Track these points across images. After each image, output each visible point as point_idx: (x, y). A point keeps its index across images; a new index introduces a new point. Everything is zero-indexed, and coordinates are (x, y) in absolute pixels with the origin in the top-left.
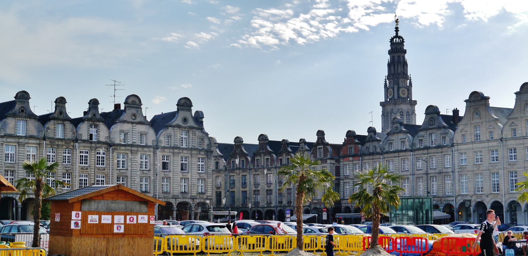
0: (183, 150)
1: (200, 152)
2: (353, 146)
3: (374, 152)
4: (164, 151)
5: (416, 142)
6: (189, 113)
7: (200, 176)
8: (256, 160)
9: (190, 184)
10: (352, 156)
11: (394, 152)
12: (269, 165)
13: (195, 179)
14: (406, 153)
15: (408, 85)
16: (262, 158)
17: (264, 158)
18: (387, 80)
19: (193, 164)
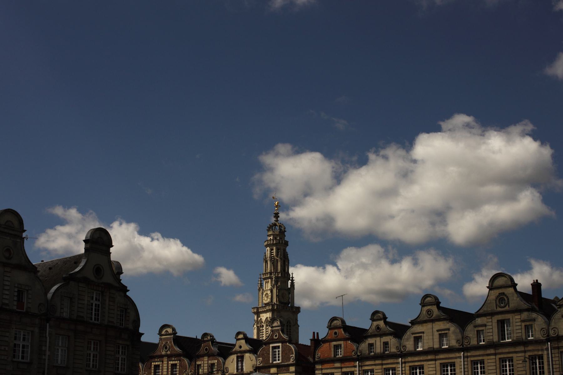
2: (342, 343)
8: (153, 366)
15: (289, 286)
16: (165, 362)
17: (168, 364)
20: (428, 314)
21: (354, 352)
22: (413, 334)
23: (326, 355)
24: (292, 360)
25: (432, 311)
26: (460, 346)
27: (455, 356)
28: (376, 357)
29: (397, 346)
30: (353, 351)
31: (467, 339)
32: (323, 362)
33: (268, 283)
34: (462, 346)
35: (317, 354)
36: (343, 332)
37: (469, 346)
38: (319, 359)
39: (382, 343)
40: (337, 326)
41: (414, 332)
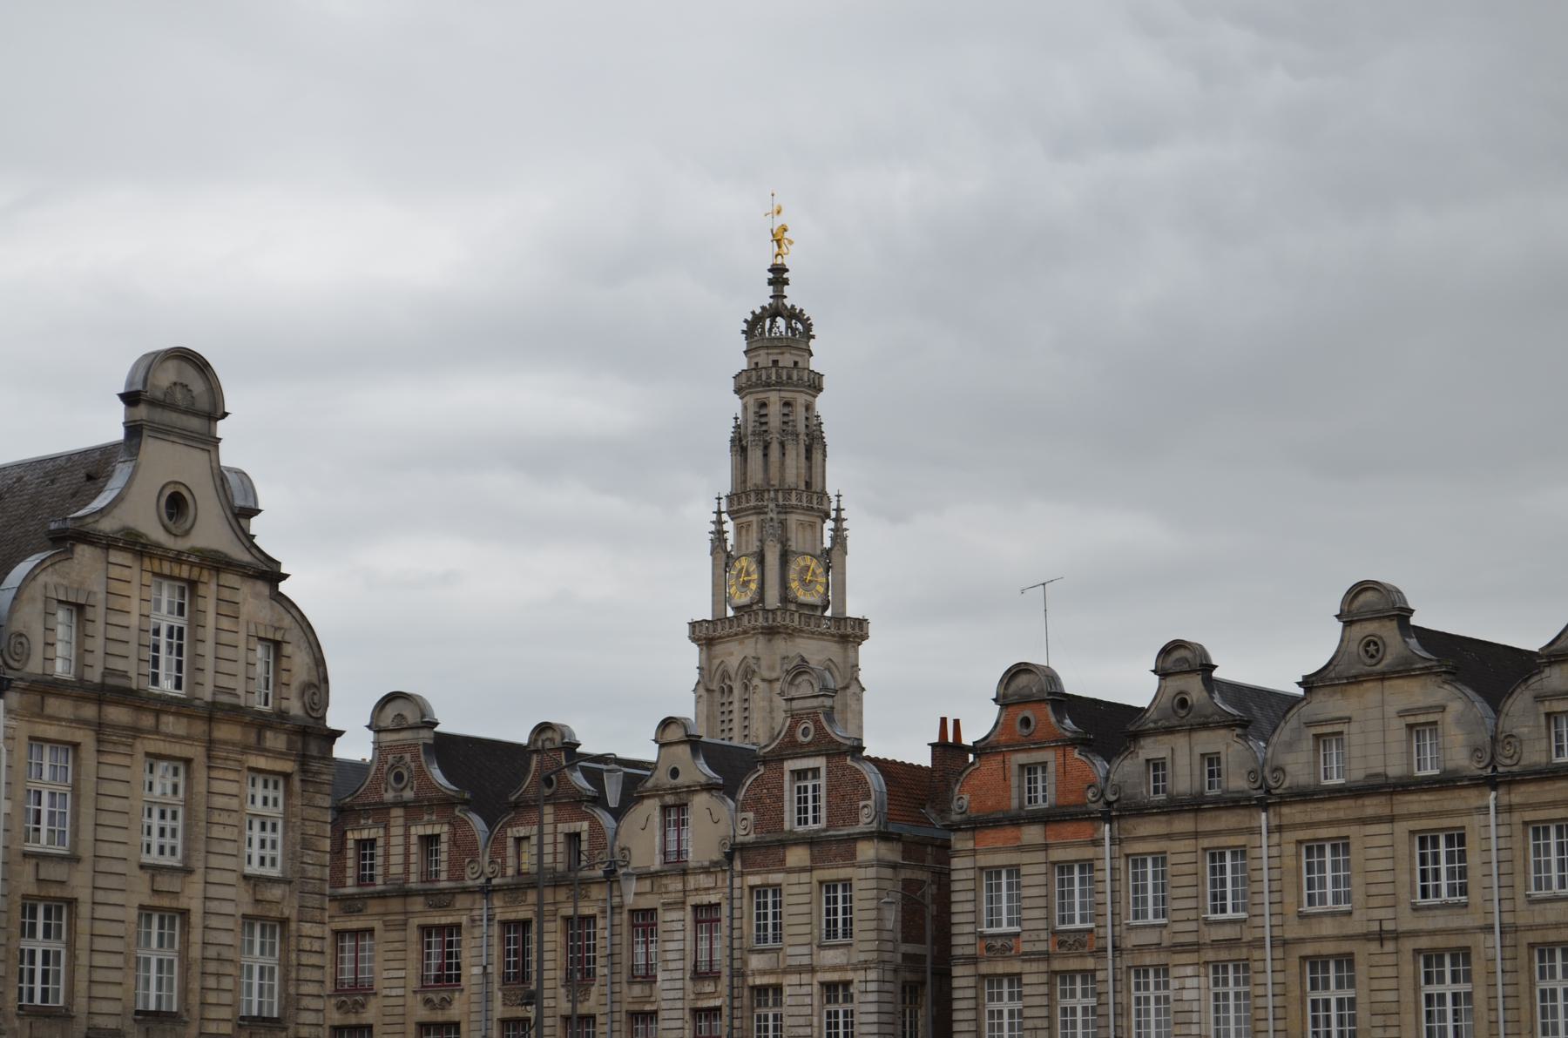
0: (158, 714)
1: (260, 738)
2: (1049, 756)
3: (1202, 793)
4: (40, 714)
6: (199, 457)
7: (257, 901)
8: (351, 844)
9: (195, 952)
10: (1045, 818)
12: (443, 876)
13: (230, 924)
14: (1448, 795)
15: (827, 544)
16: (397, 831)
17: (407, 836)
18: (725, 517)
19: (216, 818)
20: (1367, 652)
21: (1093, 789)
22: (1309, 724)
23: (989, 803)
24: (864, 820)
25: (1379, 642)
26: (1486, 767)
27: (1464, 806)
28: (1176, 807)
29: (1250, 769)
30: (1090, 787)
31: (1509, 743)
32: (976, 824)
33: (747, 531)
34: (1489, 770)
35: (956, 798)
36: (1053, 719)
37: (1515, 769)
38: (964, 816)
39: (1197, 758)
40: (1030, 696)
41: (1315, 718)
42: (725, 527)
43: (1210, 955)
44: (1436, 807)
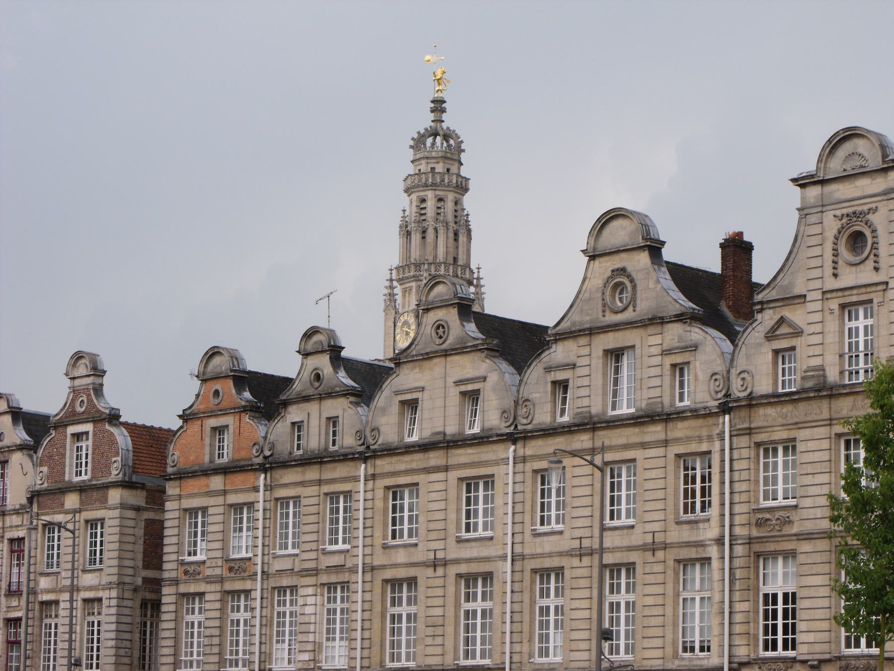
2: (228, 420)
3: (326, 449)
5: (535, 396)
10: (225, 471)
11: (424, 447)
14: (484, 448)
18: (395, 283)
20: (437, 333)
21: (257, 447)
22: (397, 393)
23: (192, 458)
24: (115, 472)
25: (445, 326)
26: (510, 426)
27: (494, 458)
28: (307, 461)
29: (357, 430)
30: (255, 444)
31: (526, 406)
32: (182, 476)
33: (409, 294)
34: (512, 428)
35: (170, 454)
36: (234, 391)
37: (529, 427)
38: (175, 468)
39: (324, 421)
40: (221, 373)
41: (401, 388)
42: (396, 291)
43: (324, 579)
44: (476, 458)
